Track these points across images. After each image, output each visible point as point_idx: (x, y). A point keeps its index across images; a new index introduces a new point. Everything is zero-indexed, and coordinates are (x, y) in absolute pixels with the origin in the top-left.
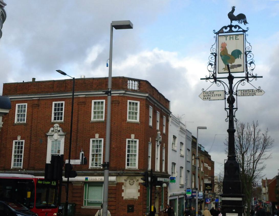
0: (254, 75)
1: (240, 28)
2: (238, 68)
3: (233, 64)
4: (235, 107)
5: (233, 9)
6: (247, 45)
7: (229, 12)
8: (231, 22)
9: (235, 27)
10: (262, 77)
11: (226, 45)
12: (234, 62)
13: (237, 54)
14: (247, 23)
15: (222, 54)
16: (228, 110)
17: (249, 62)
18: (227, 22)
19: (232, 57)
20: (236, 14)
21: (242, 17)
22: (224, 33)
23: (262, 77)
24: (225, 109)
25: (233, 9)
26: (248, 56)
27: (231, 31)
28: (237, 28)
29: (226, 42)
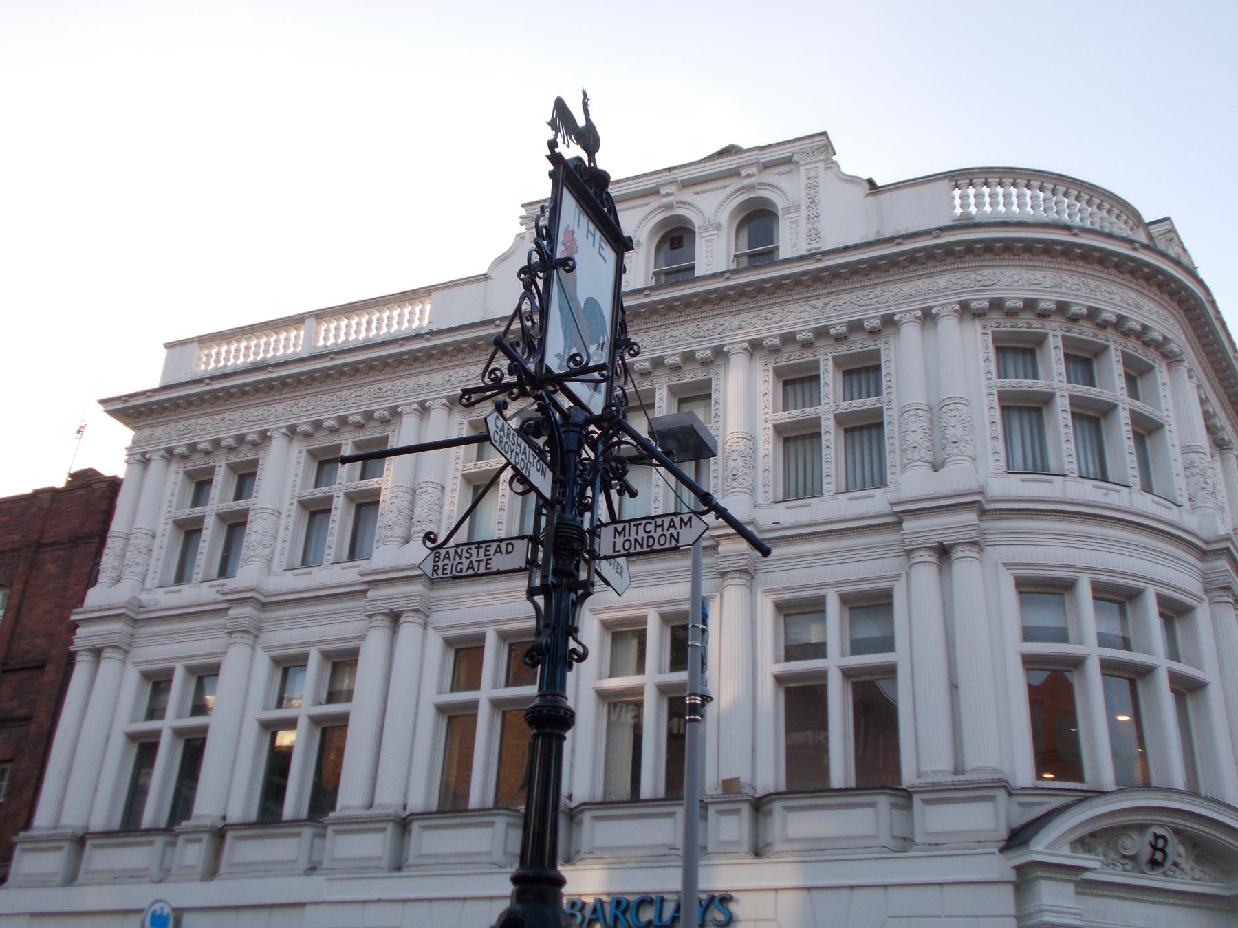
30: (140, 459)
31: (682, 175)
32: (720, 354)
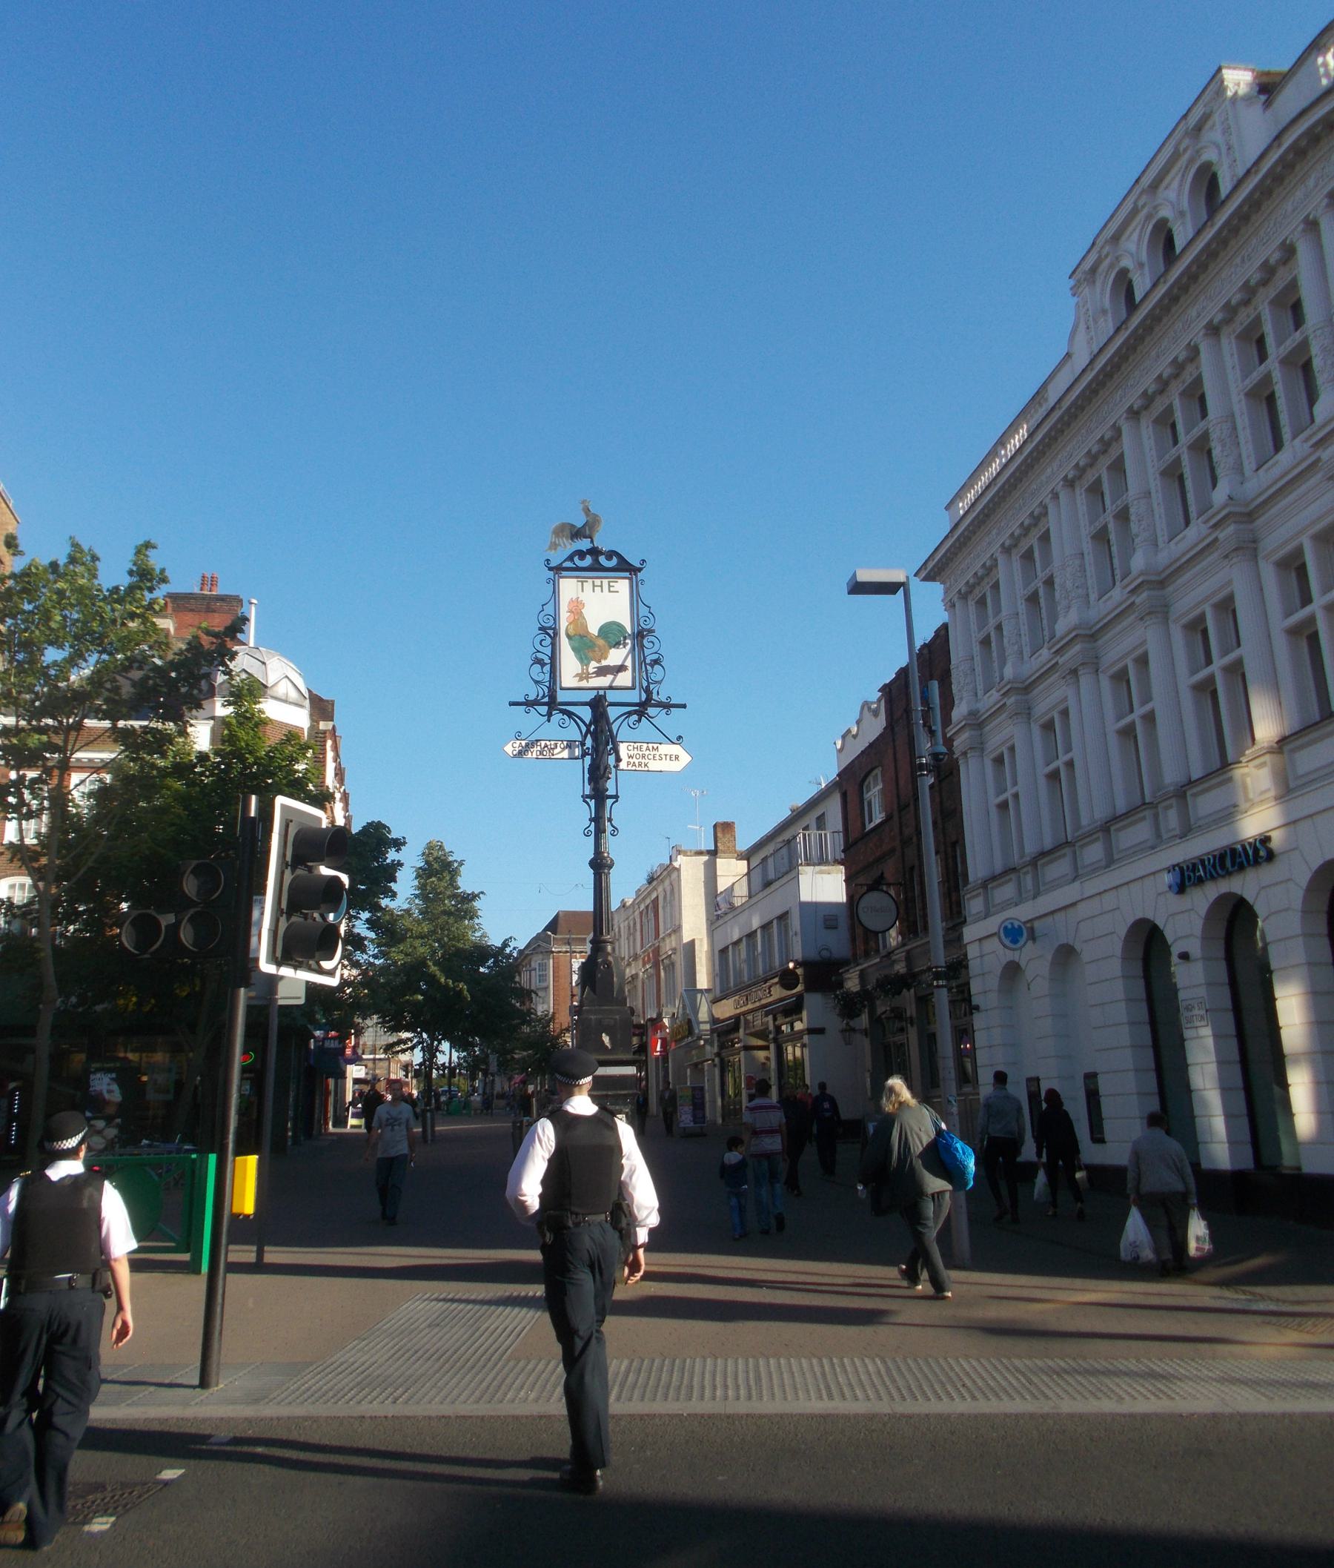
0: (663, 698)
3: (604, 663)
4: (611, 792)
6: (643, 611)
10: (684, 706)
13: (611, 634)
15: (571, 632)
16: (592, 803)
17: (648, 661)
19: (601, 642)
23: (684, 706)
24: (584, 797)
26: (645, 642)
28: (615, 559)
29: (583, 597)
30: (950, 606)
31: (1146, 181)
32: (1194, 352)
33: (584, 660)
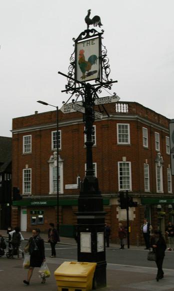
0: (110, 80)
1: (96, 31)
2: (95, 74)
3: (90, 71)
5: (89, 13)
6: (103, 48)
7: (85, 17)
8: (88, 27)
9: (92, 31)
10: (116, 82)
11: (84, 51)
12: (90, 69)
13: (92, 59)
14: (101, 25)
18: (84, 27)
20: (91, 17)
21: (97, 20)
22: (82, 39)
23: (116, 82)
25: (89, 13)
27: (88, 36)
29: (83, 48)
33: (83, 71)
